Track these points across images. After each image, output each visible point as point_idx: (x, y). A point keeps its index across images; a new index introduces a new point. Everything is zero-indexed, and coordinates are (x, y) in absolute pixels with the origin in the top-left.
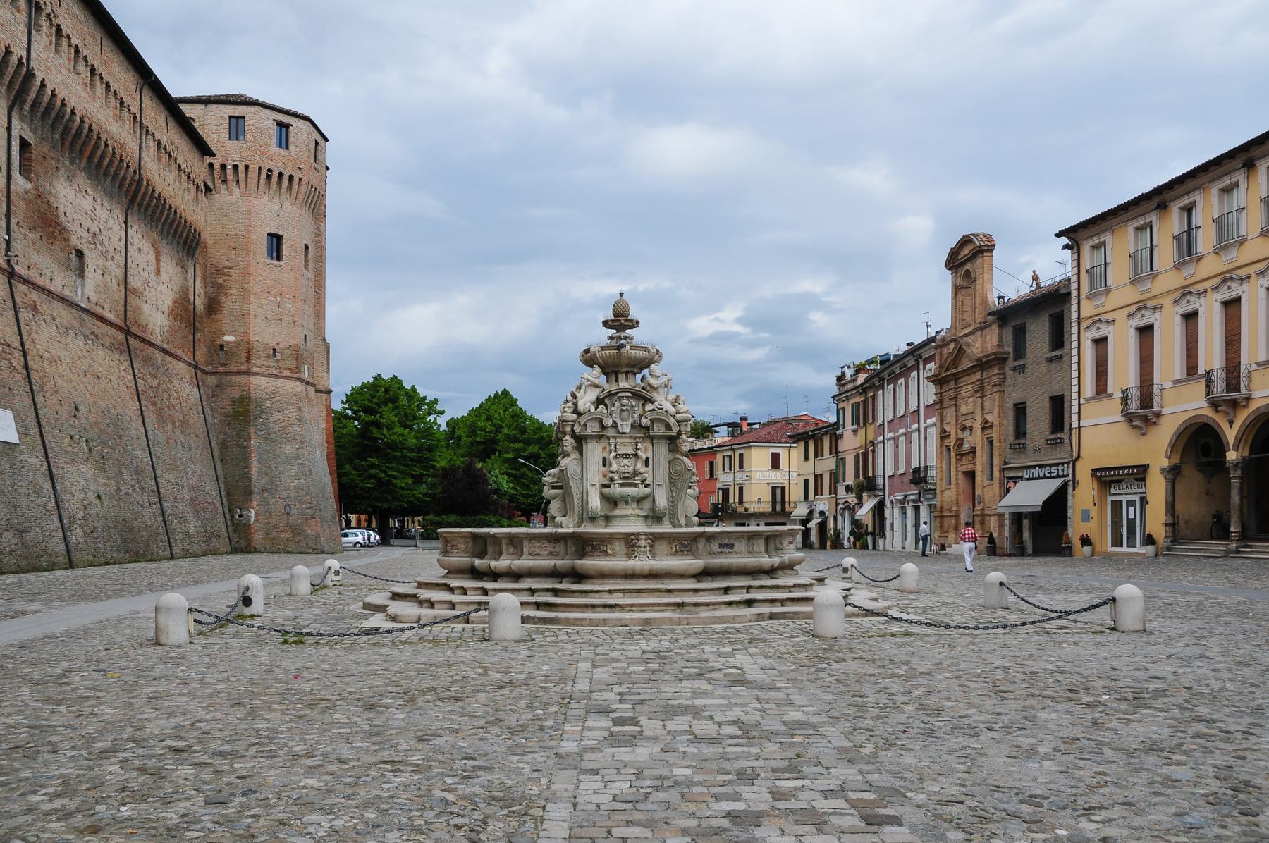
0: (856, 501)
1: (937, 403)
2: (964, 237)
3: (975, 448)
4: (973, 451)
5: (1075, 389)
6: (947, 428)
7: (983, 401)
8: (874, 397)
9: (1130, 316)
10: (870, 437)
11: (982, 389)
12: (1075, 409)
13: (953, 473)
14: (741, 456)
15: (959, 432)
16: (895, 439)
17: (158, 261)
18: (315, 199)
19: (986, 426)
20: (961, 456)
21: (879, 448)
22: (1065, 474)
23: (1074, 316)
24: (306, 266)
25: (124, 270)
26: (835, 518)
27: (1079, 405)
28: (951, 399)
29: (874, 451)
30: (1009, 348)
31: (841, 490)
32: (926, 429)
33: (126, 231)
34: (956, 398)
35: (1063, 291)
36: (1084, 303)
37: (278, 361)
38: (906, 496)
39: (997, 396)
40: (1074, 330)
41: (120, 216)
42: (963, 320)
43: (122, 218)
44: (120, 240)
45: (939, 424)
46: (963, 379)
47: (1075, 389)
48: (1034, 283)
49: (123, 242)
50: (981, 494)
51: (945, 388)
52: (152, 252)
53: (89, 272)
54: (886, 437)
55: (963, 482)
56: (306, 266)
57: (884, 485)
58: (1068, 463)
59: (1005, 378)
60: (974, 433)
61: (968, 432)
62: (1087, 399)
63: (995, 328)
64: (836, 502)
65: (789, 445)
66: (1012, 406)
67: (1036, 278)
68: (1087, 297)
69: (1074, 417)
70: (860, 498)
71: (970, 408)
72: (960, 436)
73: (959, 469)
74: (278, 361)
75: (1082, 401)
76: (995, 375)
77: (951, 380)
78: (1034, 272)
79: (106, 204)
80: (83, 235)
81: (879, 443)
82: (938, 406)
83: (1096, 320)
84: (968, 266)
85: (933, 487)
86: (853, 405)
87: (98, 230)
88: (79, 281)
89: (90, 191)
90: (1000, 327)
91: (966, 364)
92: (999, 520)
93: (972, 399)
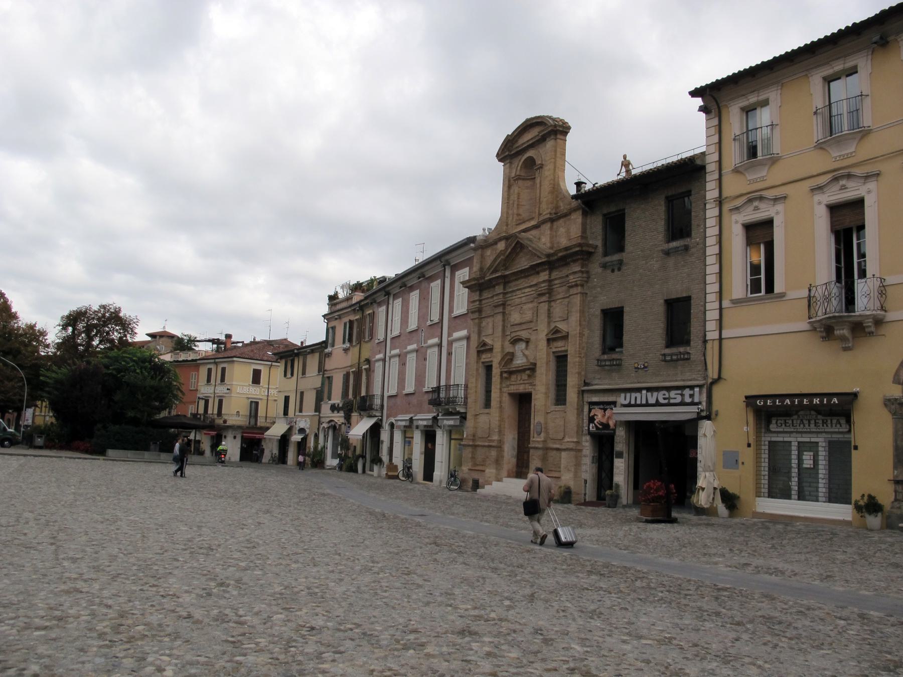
0: (342, 420)
1: (472, 312)
2: (527, 120)
3: (535, 364)
4: (532, 369)
5: (712, 288)
6: (488, 341)
7: (550, 307)
8: (372, 316)
9: (820, 189)
10: (365, 355)
11: (550, 292)
12: (712, 315)
13: (495, 394)
14: (224, 370)
15: (507, 343)
16: (402, 357)
19: (555, 336)
20: (509, 373)
21: (378, 366)
22: (696, 400)
23: (712, 193)
26: (316, 436)
27: (721, 309)
28: (495, 307)
29: (368, 371)
30: (597, 240)
31: (326, 408)
32: (450, 344)
34: (504, 305)
35: (698, 162)
36: (727, 180)
38: (411, 420)
39: (577, 300)
40: (712, 212)
42: (518, 215)
45: (474, 337)
46: (517, 282)
47: (712, 288)
48: (624, 169)
50: (542, 421)
51: (486, 294)
54: (388, 354)
55: (510, 409)
57: (382, 406)
58: (700, 386)
59: (588, 278)
60: (531, 345)
61: (523, 345)
62: (736, 302)
63: (577, 217)
64: (319, 421)
65: (270, 363)
66: (598, 312)
67: (626, 164)
68: (736, 171)
69: (711, 326)
70: (348, 418)
71: (528, 316)
72: (509, 348)
73: (505, 390)
75: (726, 303)
76: (575, 273)
77: (498, 284)
78: (625, 157)
81: (378, 360)
82: (476, 315)
83: (755, 198)
84: (530, 153)
85: (462, 410)
86: (345, 324)
90: (585, 214)
91: (523, 263)
92: (576, 457)
93: (530, 305)
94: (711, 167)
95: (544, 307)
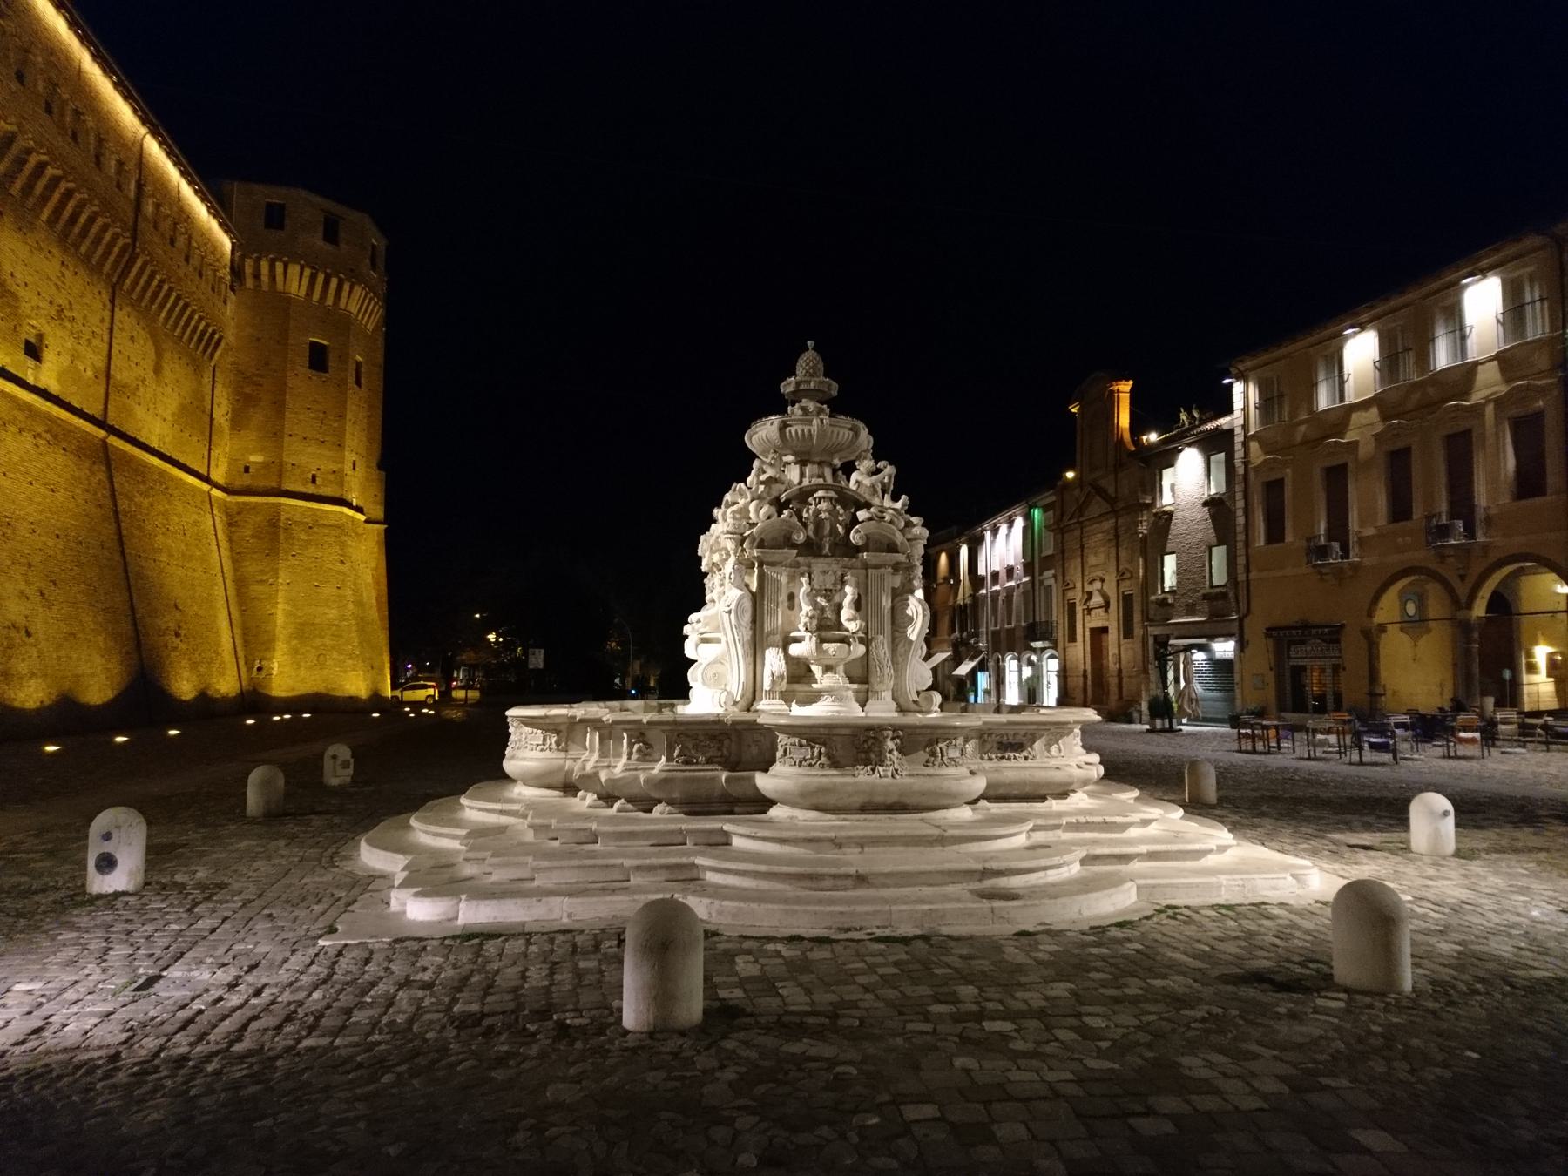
11: (1117, 536)
17: (159, 354)
18: (371, 307)
24: (358, 382)
25: (105, 361)
33: (113, 311)
37: (319, 486)
41: (104, 292)
43: (106, 297)
44: (102, 321)
45: (1060, 578)
49: (107, 324)
52: (150, 346)
53: (49, 355)
56: (358, 382)
72: (1088, 588)
74: (319, 486)
79: (82, 272)
80: (41, 304)
87: (67, 302)
88: (31, 362)
89: (55, 251)
94: (1238, 431)
95: (1113, 550)
